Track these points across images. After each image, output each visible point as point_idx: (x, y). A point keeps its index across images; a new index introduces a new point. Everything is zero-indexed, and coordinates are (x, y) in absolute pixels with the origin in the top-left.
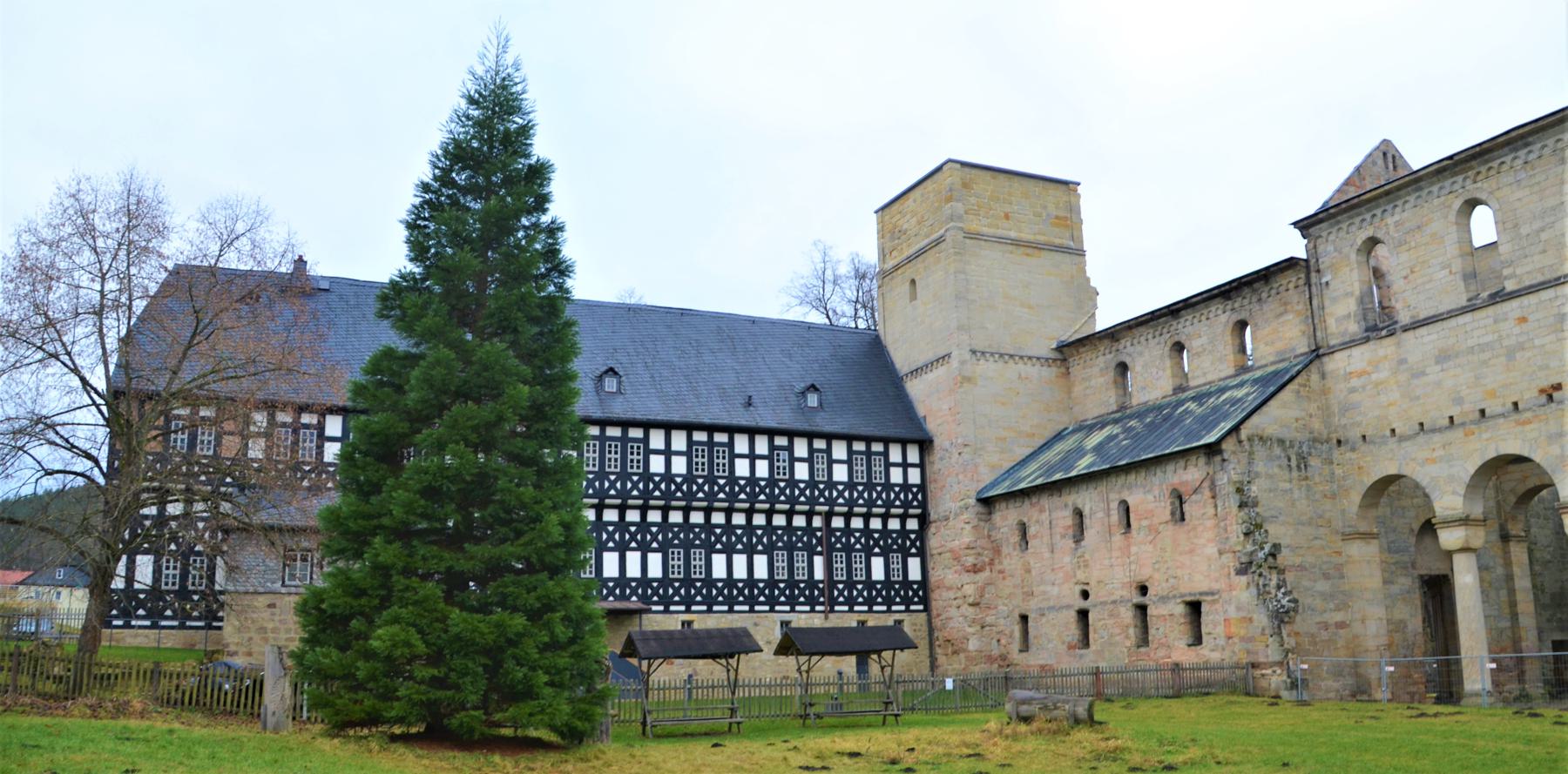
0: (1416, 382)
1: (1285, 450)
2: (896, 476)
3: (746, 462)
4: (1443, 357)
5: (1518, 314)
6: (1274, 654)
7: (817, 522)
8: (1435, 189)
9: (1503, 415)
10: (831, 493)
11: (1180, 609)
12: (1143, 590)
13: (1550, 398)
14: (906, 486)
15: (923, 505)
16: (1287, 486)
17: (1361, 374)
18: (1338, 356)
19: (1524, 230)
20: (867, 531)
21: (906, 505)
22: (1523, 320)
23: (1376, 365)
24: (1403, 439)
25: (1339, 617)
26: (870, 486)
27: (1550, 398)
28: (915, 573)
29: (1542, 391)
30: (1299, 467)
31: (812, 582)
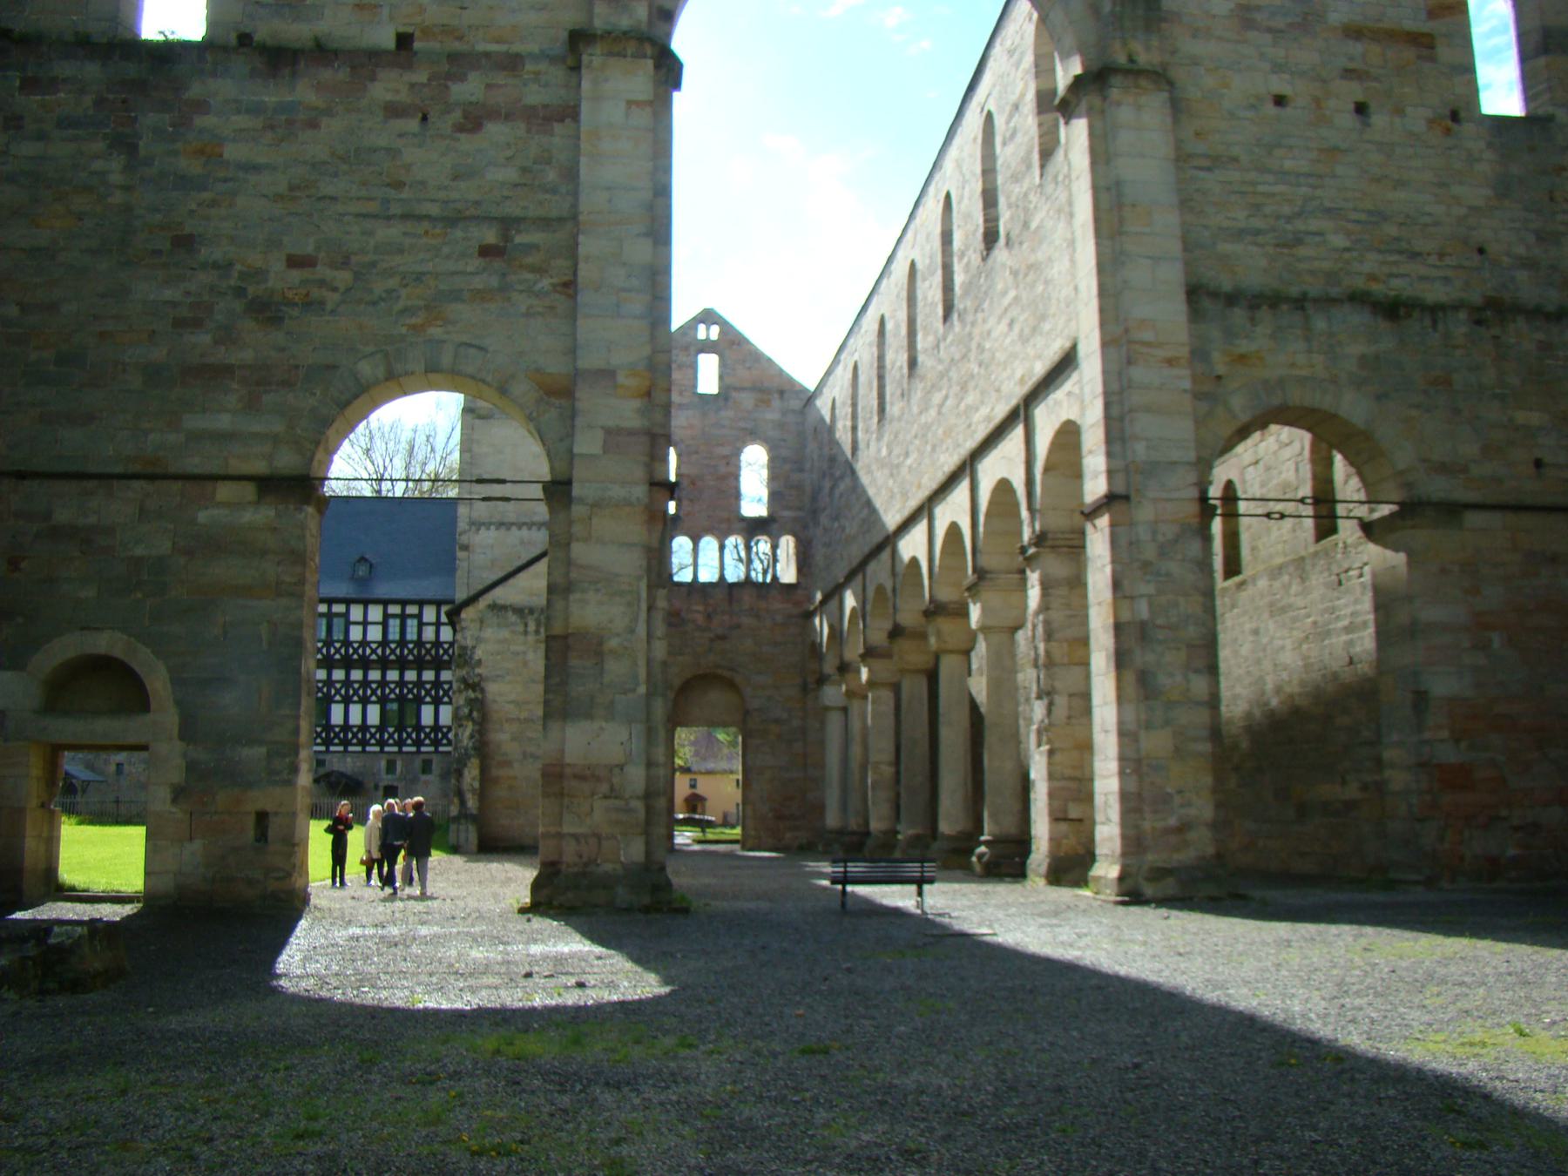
10: (364, 651)
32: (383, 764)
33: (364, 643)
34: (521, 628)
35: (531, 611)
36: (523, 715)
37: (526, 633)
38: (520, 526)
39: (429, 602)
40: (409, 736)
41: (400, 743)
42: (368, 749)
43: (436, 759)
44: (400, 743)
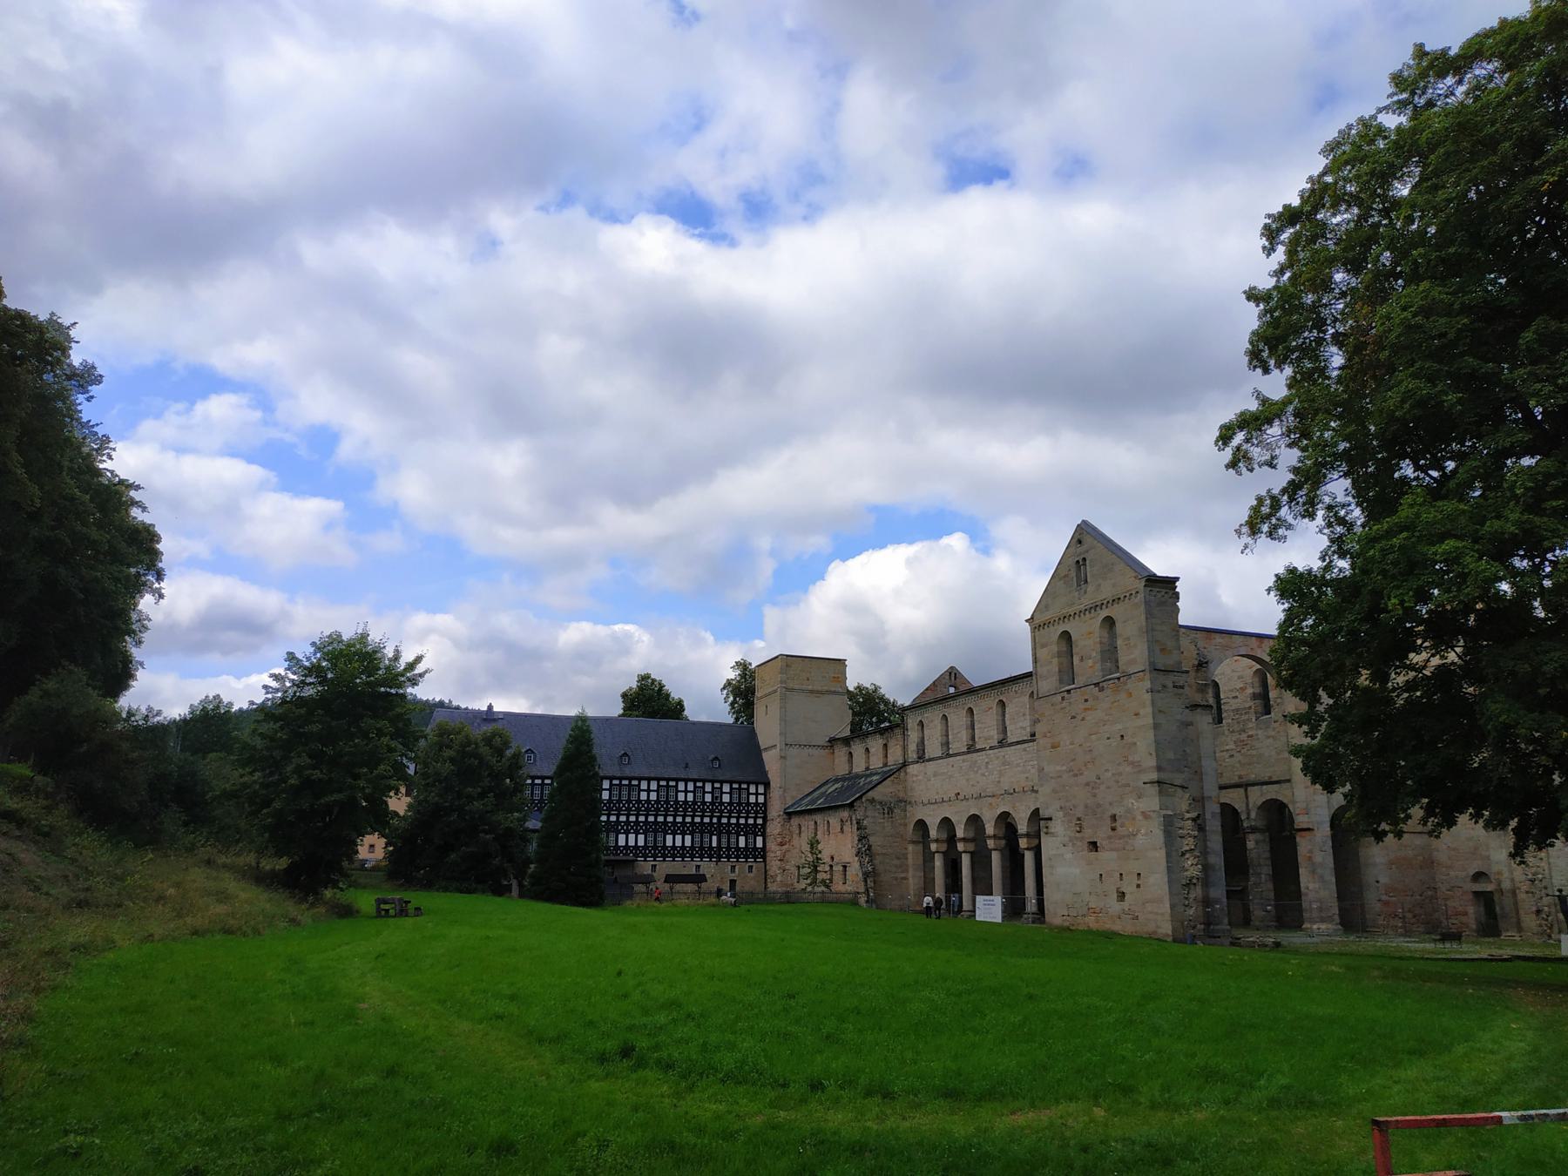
2: (752, 799)
4: (935, 775)
5: (951, 764)
7: (715, 820)
11: (841, 868)
14: (757, 804)
15: (765, 812)
16: (882, 821)
17: (917, 776)
18: (911, 766)
20: (738, 824)
21: (756, 812)
25: (903, 875)
26: (740, 804)
28: (759, 843)
30: (888, 813)
31: (711, 847)
32: (730, 867)
34: (882, 811)
36: (884, 851)
39: (753, 783)
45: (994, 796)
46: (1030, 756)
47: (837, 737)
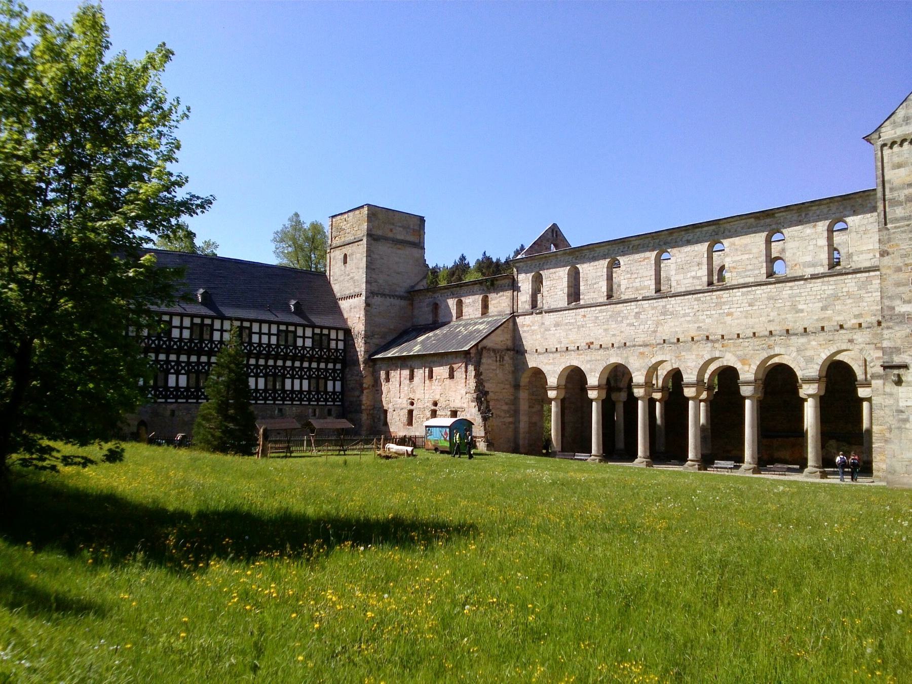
0: (547, 333)
1: (495, 354)
3: (267, 337)
4: (557, 325)
6: (483, 434)
8: (562, 259)
9: (573, 351)
12: (435, 404)
13: (589, 347)
14: (337, 350)
19: (589, 283)
22: (584, 316)
23: (533, 323)
24: (540, 354)
27: (589, 347)
28: (338, 388)
29: (587, 344)
33: (304, 347)
34: (494, 359)
35: (499, 350)
37: (496, 361)
38: (390, 296)
40: (322, 397)
41: (318, 400)
42: (303, 403)
43: (334, 409)
44: (318, 400)
45: (648, 345)
46: (705, 305)
47: (416, 288)
